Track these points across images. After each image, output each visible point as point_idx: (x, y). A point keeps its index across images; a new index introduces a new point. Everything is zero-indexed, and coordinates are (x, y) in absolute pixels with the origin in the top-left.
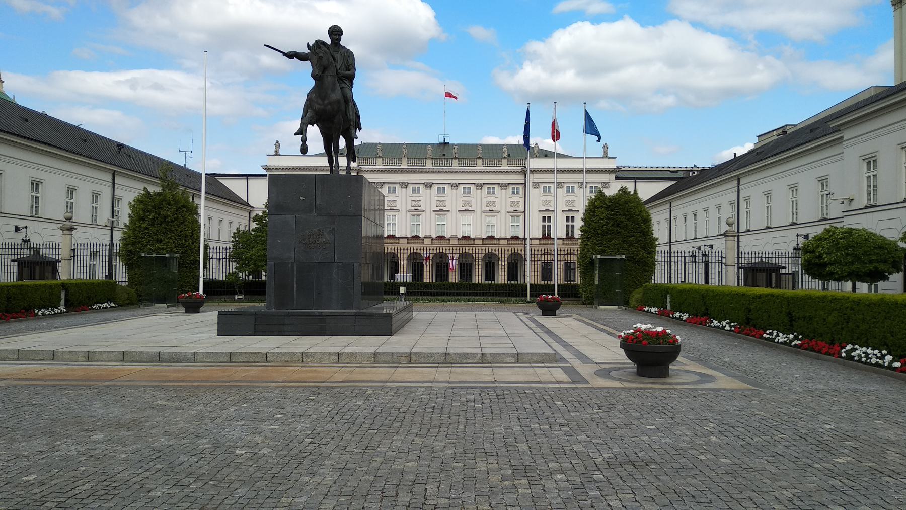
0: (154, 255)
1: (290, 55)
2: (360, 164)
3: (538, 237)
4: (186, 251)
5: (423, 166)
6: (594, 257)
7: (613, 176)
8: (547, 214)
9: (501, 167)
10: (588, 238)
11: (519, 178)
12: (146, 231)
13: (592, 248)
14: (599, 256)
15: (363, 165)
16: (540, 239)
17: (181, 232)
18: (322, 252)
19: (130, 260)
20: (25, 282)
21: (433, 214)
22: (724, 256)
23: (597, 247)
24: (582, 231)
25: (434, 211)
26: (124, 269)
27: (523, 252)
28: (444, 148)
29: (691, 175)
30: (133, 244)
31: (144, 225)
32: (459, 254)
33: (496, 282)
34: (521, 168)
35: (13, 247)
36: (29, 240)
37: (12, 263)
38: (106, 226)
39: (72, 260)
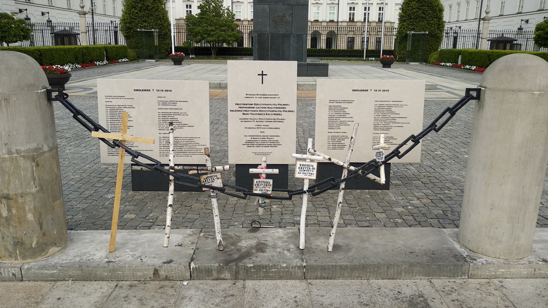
0: (143, 30)
3: (390, 21)
4: (161, 27)
6: (408, 32)
8: (352, 6)
10: (404, 21)
12: (137, 15)
13: (406, 27)
14: (413, 32)
16: (347, 22)
17: (157, 15)
19: (128, 33)
20: (58, 47)
22: (481, 33)
23: (410, 26)
24: (400, 16)
26: (123, 38)
27: (336, 30)
30: (130, 23)
31: (136, 11)
35: (39, 25)
36: (51, 21)
38: (89, 12)
39: (88, 33)
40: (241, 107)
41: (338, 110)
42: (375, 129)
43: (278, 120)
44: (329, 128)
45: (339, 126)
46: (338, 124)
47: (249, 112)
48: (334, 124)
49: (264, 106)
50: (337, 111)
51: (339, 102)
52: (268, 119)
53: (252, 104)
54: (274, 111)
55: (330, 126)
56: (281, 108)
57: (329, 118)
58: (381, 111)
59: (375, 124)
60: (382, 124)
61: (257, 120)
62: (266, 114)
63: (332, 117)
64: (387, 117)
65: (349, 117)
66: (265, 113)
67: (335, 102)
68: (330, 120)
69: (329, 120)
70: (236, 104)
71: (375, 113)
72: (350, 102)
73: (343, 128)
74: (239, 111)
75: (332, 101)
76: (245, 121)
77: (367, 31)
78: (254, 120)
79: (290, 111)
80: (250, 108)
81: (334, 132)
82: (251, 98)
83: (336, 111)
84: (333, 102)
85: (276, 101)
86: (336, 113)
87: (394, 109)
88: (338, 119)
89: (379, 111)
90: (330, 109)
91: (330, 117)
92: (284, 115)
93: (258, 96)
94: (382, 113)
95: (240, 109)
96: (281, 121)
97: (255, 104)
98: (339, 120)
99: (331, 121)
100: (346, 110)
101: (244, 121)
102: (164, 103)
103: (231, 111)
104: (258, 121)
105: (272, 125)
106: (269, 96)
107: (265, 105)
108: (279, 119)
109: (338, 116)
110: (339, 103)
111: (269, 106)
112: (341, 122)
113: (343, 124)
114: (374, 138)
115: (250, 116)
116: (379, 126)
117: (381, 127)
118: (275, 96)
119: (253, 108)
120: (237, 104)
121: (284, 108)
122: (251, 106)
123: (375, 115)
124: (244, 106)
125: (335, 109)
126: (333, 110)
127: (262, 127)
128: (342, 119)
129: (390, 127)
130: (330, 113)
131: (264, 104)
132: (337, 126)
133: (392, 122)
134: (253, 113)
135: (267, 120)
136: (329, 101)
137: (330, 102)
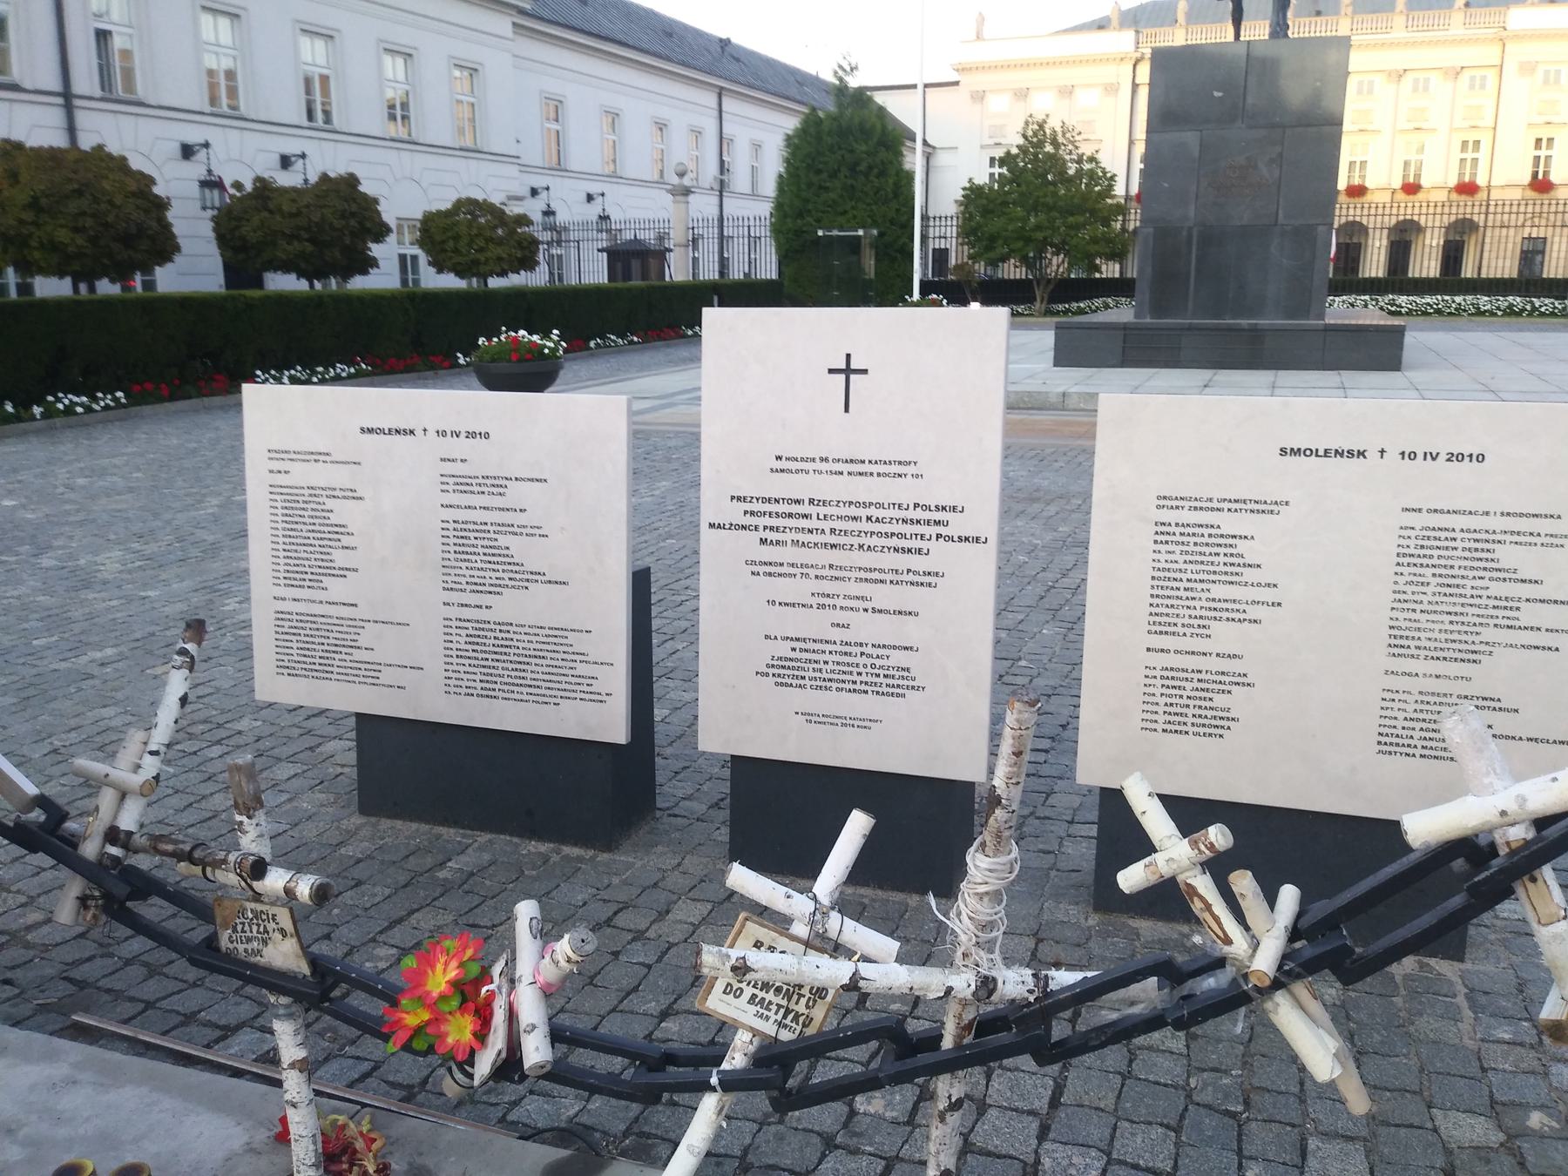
40: (752, 513)
41: (1202, 544)
42: (1396, 651)
43: (911, 577)
44: (1154, 628)
45: (1202, 622)
46: (1198, 613)
47: (788, 537)
48: (1181, 612)
49: (853, 511)
50: (1198, 549)
51: (1209, 505)
52: (866, 570)
53: (798, 502)
54: (893, 534)
55: (1158, 619)
56: (928, 522)
57: (1156, 583)
58: (1435, 561)
59: (1399, 628)
60: (1437, 627)
61: (819, 572)
62: (861, 547)
63: (1172, 575)
64: (1469, 592)
65: (1259, 585)
66: (856, 541)
67: (1187, 504)
68: (1160, 592)
69: (1155, 592)
70: (733, 498)
71: (1400, 569)
72: (1264, 508)
73: (1224, 636)
74: (744, 527)
75: (1170, 498)
76: (770, 574)
78: (805, 571)
79: (967, 539)
80: (790, 515)
81: (1177, 652)
82: (797, 471)
83: (1191, 548)
84: (1175, 503)
85: (903, 491)
86: (1189, 558)
87: (1507, 555)
88: (1199, 586)
89: (1425, 561)
90: (1159, 538)
91: (1159, 579)
92: (940, 555)
93: (824, 466)
94: (1437, 571)
95: (749, 520)
96: (928, 580)
97: (811, 501)
98: (1204, 595)
99: (1164, 597)
100: (1242, 547)
101: (766, 574)
102: (464, 484)
103: (712, 526)
104: (823, 578)
105: (884, 596)
106: (875, 469)
107: (858, 504)
108: (916, 573)
109: (1201, 576)
110: (1207, 509)
111: (873, 512)
112: (1213, 605)
113: (1225, 615)
114: (1388, 696)
115: (787, 554)
116: (1422, 635)
117: (1432, 645)
118: (901, 468)
119: (805, 516)
120: (739, 499)
121: (937, 523)
122: (795, 509)
123: (1401, 580)
124: (767, 507)
125: (1185, 539)
126: (1177, 543)
127: (840, 602)
128: (1219, 591)
129: (1482, 648)
130: (1163, 557)
131: (851, 503)
132: (1196, 622)
133: (1492, 622)
134: (801, 537)
135: (863, 575)
136: (1159, 498)
137: (1162, 502)
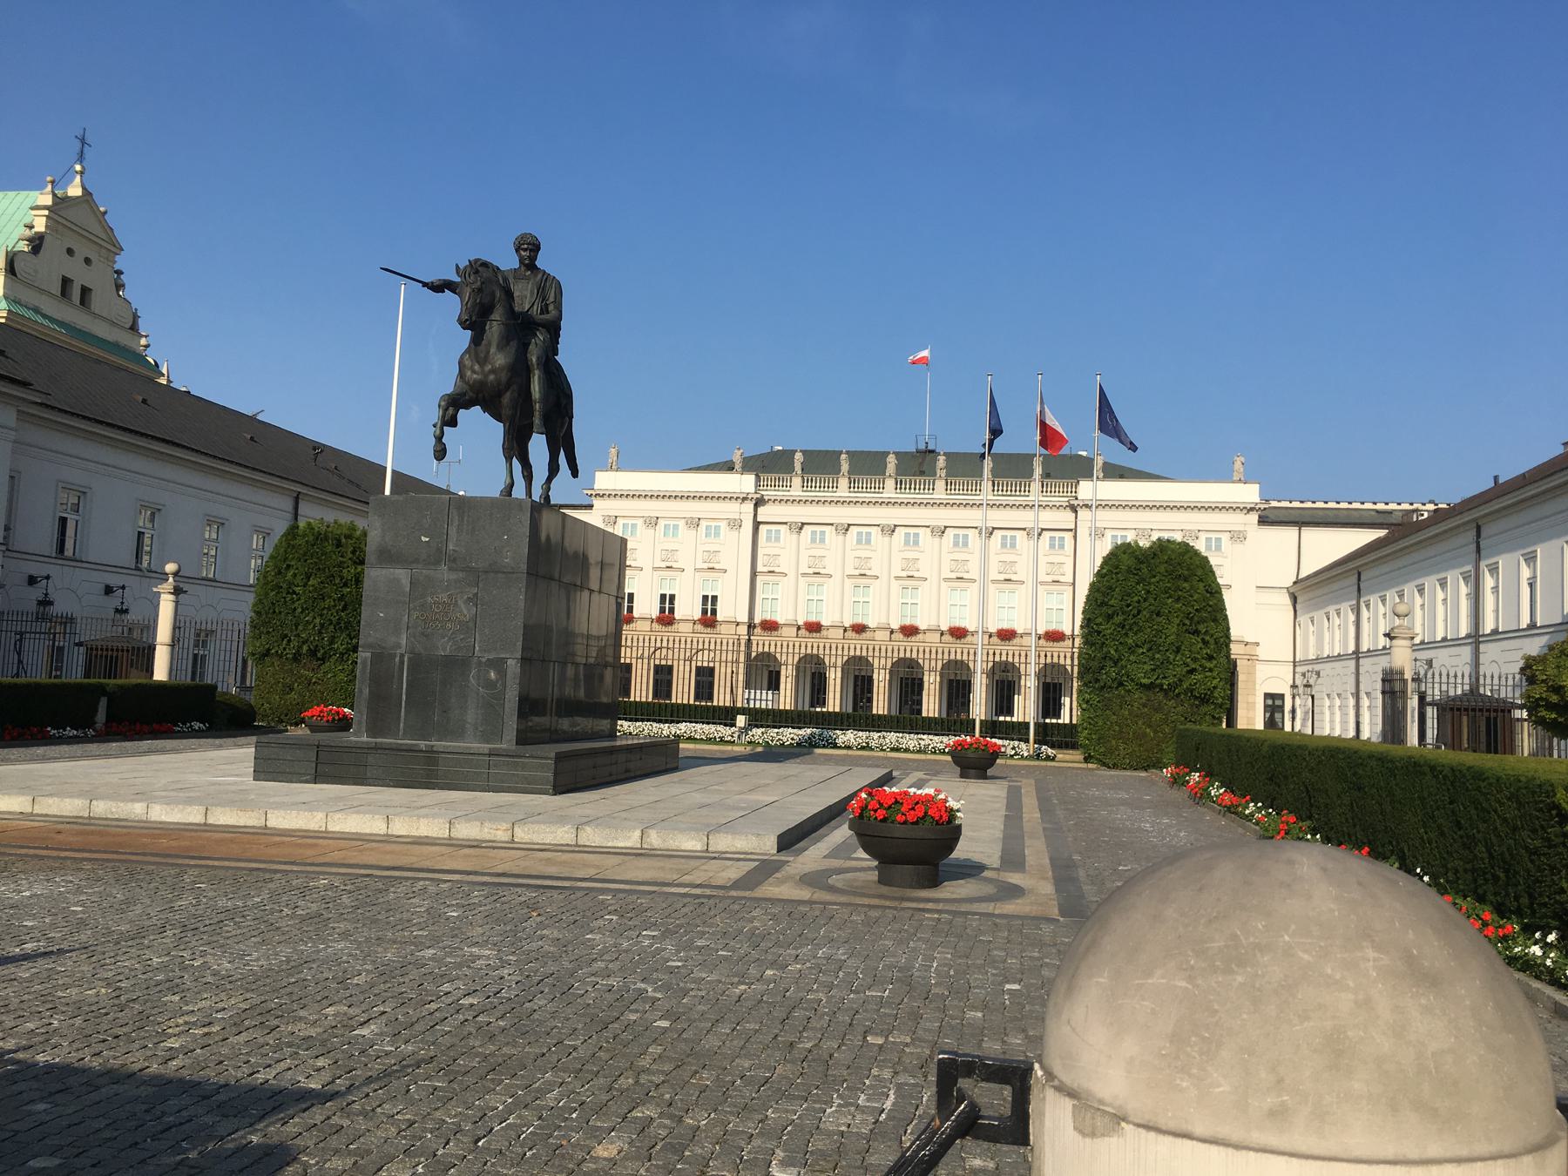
1: (438, 287)
2: (761, 488)
5: (878, 493)
7: (1254, 517)
9: (1028, 496)
11: (1066, 519)
15: (766, 490)
18: (454, 636)
21: (895, 585)
25: (897, 578)
28: (924, 460)
29: (1415, 519)
32: (800, 654)
33: (715, 703)
34: (1067, 499)
37: (76, 648)
77: (982, 661)
